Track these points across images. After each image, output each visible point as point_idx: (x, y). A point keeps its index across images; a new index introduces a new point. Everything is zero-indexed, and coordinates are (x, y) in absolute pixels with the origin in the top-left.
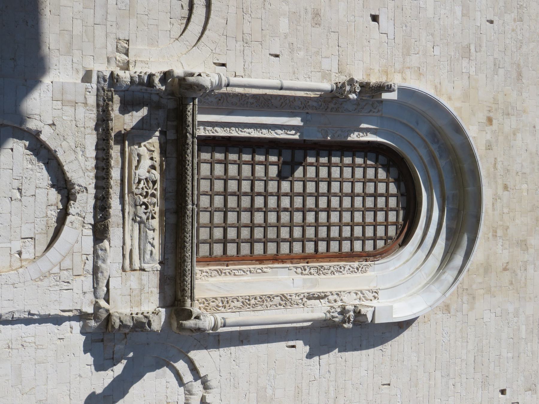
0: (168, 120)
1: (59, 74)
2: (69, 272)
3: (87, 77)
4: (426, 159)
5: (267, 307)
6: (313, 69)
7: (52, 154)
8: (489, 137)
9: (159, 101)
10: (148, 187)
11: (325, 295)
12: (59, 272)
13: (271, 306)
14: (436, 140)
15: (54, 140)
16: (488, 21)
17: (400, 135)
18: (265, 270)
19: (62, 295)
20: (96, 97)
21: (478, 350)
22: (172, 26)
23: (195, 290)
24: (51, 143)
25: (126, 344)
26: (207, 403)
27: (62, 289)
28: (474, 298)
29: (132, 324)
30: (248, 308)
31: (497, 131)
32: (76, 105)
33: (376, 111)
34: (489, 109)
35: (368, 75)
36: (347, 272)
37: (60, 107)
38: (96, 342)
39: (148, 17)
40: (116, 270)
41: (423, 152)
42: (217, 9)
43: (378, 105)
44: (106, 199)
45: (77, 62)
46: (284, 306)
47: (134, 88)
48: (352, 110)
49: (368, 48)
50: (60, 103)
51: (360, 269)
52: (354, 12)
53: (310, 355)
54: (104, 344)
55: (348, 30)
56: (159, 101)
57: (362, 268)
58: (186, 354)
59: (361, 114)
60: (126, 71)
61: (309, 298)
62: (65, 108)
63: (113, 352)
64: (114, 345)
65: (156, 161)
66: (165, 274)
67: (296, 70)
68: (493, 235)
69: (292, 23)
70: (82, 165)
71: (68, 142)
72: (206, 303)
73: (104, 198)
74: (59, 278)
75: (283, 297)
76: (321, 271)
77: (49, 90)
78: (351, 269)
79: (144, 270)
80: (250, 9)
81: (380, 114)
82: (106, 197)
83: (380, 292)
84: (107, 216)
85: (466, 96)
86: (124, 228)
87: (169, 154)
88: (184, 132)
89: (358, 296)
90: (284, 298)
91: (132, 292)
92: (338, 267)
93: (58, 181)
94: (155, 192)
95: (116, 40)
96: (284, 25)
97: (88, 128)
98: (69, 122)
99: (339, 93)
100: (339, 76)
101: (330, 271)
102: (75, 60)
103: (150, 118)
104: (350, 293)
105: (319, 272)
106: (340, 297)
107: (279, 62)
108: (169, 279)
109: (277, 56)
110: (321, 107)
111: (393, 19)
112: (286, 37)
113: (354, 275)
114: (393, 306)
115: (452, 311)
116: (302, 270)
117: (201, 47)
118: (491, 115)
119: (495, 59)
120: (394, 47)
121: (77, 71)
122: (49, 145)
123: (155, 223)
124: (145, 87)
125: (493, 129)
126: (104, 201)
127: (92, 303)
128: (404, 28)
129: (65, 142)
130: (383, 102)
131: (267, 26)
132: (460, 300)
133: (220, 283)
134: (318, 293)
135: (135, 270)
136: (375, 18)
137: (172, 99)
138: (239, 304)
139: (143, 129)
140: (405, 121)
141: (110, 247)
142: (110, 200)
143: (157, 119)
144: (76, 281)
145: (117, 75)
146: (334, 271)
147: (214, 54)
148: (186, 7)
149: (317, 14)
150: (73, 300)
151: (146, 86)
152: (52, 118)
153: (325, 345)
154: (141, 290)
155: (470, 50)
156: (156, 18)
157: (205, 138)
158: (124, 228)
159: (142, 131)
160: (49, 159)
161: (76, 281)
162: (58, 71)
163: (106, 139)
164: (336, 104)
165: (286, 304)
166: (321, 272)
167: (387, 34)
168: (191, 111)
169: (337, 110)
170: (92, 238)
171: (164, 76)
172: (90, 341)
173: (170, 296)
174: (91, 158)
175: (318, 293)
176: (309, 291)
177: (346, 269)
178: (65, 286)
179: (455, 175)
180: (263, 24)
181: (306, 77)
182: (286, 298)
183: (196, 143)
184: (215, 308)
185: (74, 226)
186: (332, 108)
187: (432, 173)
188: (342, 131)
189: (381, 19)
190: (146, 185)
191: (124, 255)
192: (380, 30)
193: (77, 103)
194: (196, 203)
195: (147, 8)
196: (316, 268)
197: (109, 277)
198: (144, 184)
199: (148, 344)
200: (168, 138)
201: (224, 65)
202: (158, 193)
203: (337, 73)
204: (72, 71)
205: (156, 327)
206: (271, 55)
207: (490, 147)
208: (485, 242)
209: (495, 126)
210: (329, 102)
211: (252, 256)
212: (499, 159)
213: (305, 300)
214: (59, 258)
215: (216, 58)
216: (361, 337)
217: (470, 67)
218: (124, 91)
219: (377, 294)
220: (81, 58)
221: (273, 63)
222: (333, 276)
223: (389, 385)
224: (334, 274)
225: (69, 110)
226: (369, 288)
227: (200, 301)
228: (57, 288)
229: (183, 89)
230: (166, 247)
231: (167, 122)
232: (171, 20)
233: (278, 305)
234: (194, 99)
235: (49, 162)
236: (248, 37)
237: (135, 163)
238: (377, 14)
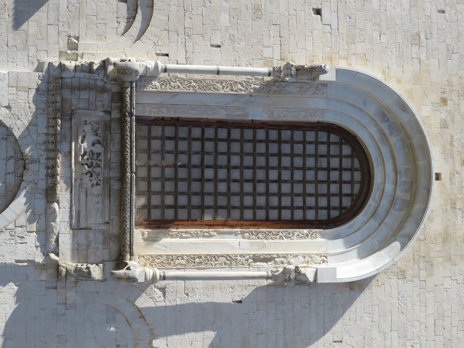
0: (112, 102)
1: (16, 66)
2: (23, 228)
3: (39, 69)
4: (377, 137)
5: (212, 266)
6: (254, 57)
7: (10, 131)
8: (443, 116)
9: (104, 86)
10: (93, 158)
11: (272, 257)
12: (14, 228)
13: (216, 265)
14: (386, 119)
15: (9, 119)
16: (439, 11)
17: (348, 115)
18: (212, 233)
19: (16, 247)
21: (439, 314)
22: (118, 24)
23: (134, 247)
24: (7, 122)
25: (76, 292)
26: (154, 347)
27: (17, 242)
28: (432, 265)
30: (193, 266)
31: (453, 111)
32: (30, 90)
33: (320, 93)
34: (442, 90)
35: (311, 61)
36: (296, 237)
38: (50, 289)
39: (97, 17)
40: (65, 228)
41: (373, 130)
42: (159, 8)
43: (323, 87)
44: (55, 168)
45: (32, 56)
46: (229, 265)
47: (78, 74)
48: (296, 92)
49: (311, 38)
51: (310, 235)
52: (296, 6)
53: (257, 310)
54: (57, 291)
55: (290, 22)
56: (104, 86)
57: (312, 234)
58: (133, 303)
59: (304, 96)
60: (72, 61)
62: (19, 93)
63: (66, 298)
64: (66, 292)
65: (100, 137)
66: (110, 233)
67: (238, 58)
68: (452, 207)
69: (232, 18)
71: (22, 121)
72: (151, 259)
74: (14, 233)
75: (228, 257)
76: (270, 236)
77: (6, 78)
78: (301, 235)
80: (191, 7)
81: (325, 95)
82: (55, 166)
83: (329, 257)
84: (55, 181)
85: (416, 80)
87: (113, 130)
89: (306, 259)
90: (229, 258)
91: (80, 247)
92: (286, 233)
93: (15, 153)
94: (99, 163)
95: (67, 38)
96: (225, 19)
97: (40, 109)
98: (23, 105)
99: (277, 76)
100: (281, 62)
101: (278, 237)
102: (30, 54)
103: (96, 100)
104: (297, 256)
105: (267, 236)
106: (287, 259)
107: (220, 52)
108: (114, 237)
109: (219, 46)
110: (264, 90)
111: (336, 11)
112: (227, 30)
113: (304, 240)
114: (337, 268)
115: (408, 277)
116: (250, 235)
117: (144, 40)
118: (445, 96)
119: (447, 45)
120: (338, 36)
121: (33, 63)
122: (5, 123)
124: (87, 74)
125: (448, 109)
126: (53, 169)
128: (348, 19)
129: (19, 121)
130: (328, 85)
131: (208, 21)
132: (416, 266)
133: (166, 243)
134: (264, 255)
136: (318, 12)
137: (116, 84)
138: (184, 262)
139: (89, 110)
140: (351, 102)
141: (59, 208)
142: (57, 168)
143: (102, 101)
144: (29, 236)
146: (283, 236)
147: (157, 46)
149: (257, 9)
150: (26, 252)
151: (87, 73)
152: (8, 101)
153: (272, 302)
154: (88, 246)
155: (419, 37)
156: (104, 18)
157: (154, 119)
159: (87, 111)
160: (7, 135)
161: (29, 236)
162: (15, 63)
163: (55, 117)
164: (278, 87)
165: (231, 264)
166: (269, 237)
167: (330, 25)
168: (129, 93)
169: (280, 93)
171: (103, 64)
172: (45, 288)
173: (115, 251)
175: (264, 255)
177: (295, 235)
179: (408, 151)
180: (204, 19)
181: (247, 64)
182: (232, 258)
183: (134, 120)
184: (160, 264)
186: (276, 91)
187: (384, 150)
188: (288, 112)
189: (323, 12)
190: (91, 156)
192: (323, 22)
193: (30, 89)
194: (134, 171)
195: (95, 10)
196: (264, 233)
197: (59, 233)
198: (89, 155)
199: (97, 293)
200: (112, 117)
201: (167, 55)
203: (279, 60)
204: (28, 64)
205: (96, 277)
206: (212, 46)
207: (445, 126)
208: (443, 213)
210: (272, 86)
211: (202, 221)
212: (455, 137)
213: (251, 260)
214: (14, 216)
215: (159, 50)
216: (310, 296)
217: (421, 53)
218: (71, 78)
219: (326, 258)
220: (36, 52)
221: (214, 52)
222: (282, 241)
223: (341, 342)
224: (283, 239)
226: (318, 252)
227: (146, 257)
228: (12, 241)
229: (120, 74)
230: (111, 209)
231: (111, 104)
232: (118, 19)
233: (223, 264)
234: (131, 82)
235: (8, 137)
238: (320, 7)
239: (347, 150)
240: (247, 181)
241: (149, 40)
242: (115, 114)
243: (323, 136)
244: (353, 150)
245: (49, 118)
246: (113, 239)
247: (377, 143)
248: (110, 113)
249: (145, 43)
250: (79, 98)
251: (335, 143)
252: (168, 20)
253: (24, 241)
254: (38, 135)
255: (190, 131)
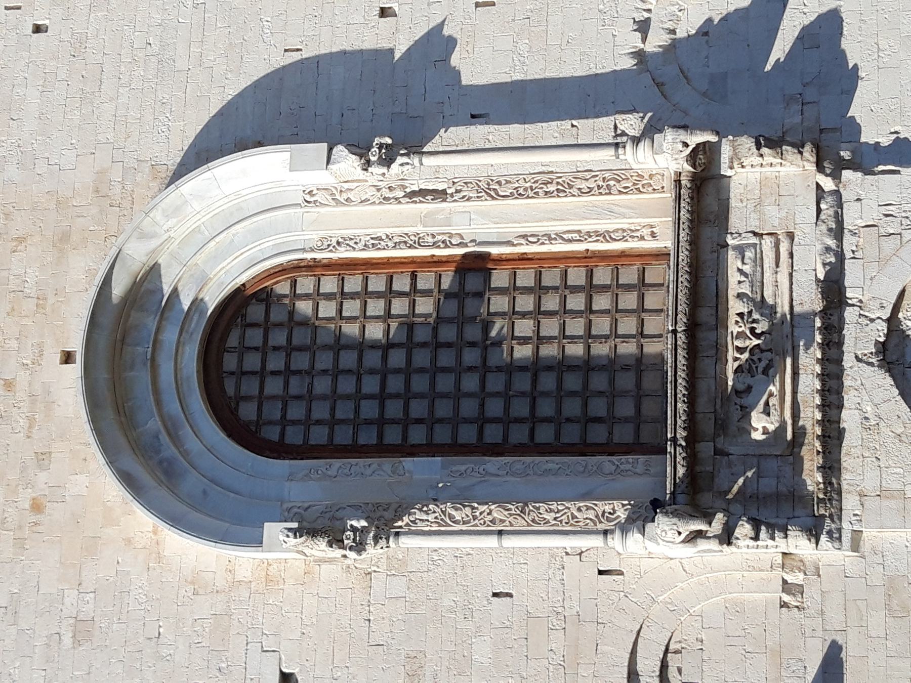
4: (186, 431)
5: (525, 179)
8: (43, 477)
10: (751, 362)
11: (410, 199)
12: (903, 232)
14: (165, 464)
20: (843, 507)
29: (784, 147)
30: (560, 177)
31: (20, 487)
32: (878, 493)
33: (296, 510)
34: (38, 529)
36: (360, 240)
41: (192, 443)
44: (825, 343)
46: (492, 180)
61: (444, 192)
65: (736, 404)
70: (866, 398)
71: (893, 432)
73: (828, 345)
74: (903, 223)
75: (495, 196)
76: (412, 240)
78: (351, 243)
79: (755, 234)
81: (285, 506)
82: (825, 346)
83: (300, 201)
84: (823, 317)
90: (492, 193)
96: (482, 651)
109: (495, 595)
116: (450, 241)
119: (15, 624)
123: (736, 307)
125: (30, 491)
126: (827, 340)
131: (516, 646)
135: (768, 234)
145: (810, 540)
147: (622, 590)
148: (672, 673)
150: (878, 189)
154: (759, 204)
155: (74, 636)
156: (729, 648)
163: (827, 439)
165: (488, 184)
166: (413, 238)
169: (378, 505)
170: (847, 282)
176: (444, 205)
178: (892, 210)
179: (125, 405)
181: (439, 561)
184: (621, 178)
185: (878, 301)
187: (173, 407)
190: (754, 366)
191: (791, 255)
196: (422, 244)
198: (757, 367)
201: (601, 572)
202: (731, 354)
203: (375, 571)
206: (510, 595)
207: (41, 457)
209: (25, 499)
217: (75, 604)
218: (794, 517)
219: (305, 200)
220: (868, 573)
223: (286, 51)
227: (650, 189)
232: (700, 647)
233: (504, 182)
236: (558, 623)
239: (248, 411)
240: (449, 345)
241: (638, 603)
242: (705, 449)
243: (294, 436)
244: (234, 412)
246: (712, 217)
247: (187, 420)
248: (717, 452)
249: (646, 595)
250: (778, 478)
251: (270, 423)
252: (597, 645)
255: (558, 435)
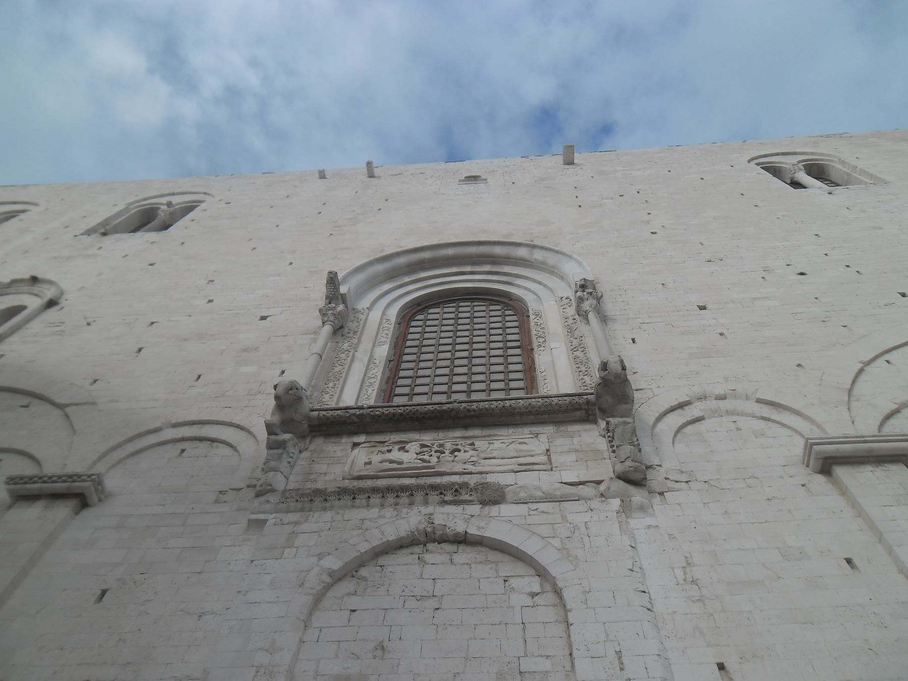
37: (295, 550)
50: (287, 551)
62: (296, 544)
79: (548, 450)
86: (487, 473)
88: (355, 419)
127: (603, 501)
158: (487, 473)
174: (379, 512)
197: (562, 483)
225: (300, 540)
237: (395, 466)
245: (353, 507)
253: (582, 526)
254: (383, 517)
